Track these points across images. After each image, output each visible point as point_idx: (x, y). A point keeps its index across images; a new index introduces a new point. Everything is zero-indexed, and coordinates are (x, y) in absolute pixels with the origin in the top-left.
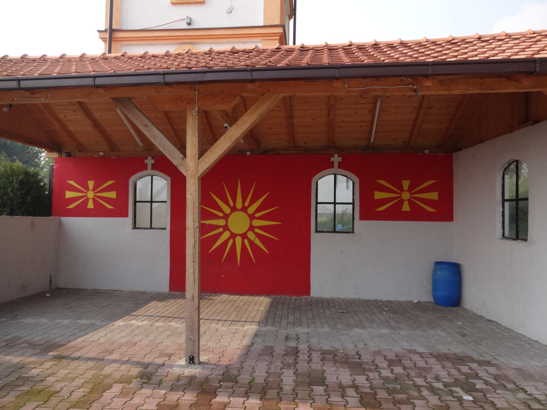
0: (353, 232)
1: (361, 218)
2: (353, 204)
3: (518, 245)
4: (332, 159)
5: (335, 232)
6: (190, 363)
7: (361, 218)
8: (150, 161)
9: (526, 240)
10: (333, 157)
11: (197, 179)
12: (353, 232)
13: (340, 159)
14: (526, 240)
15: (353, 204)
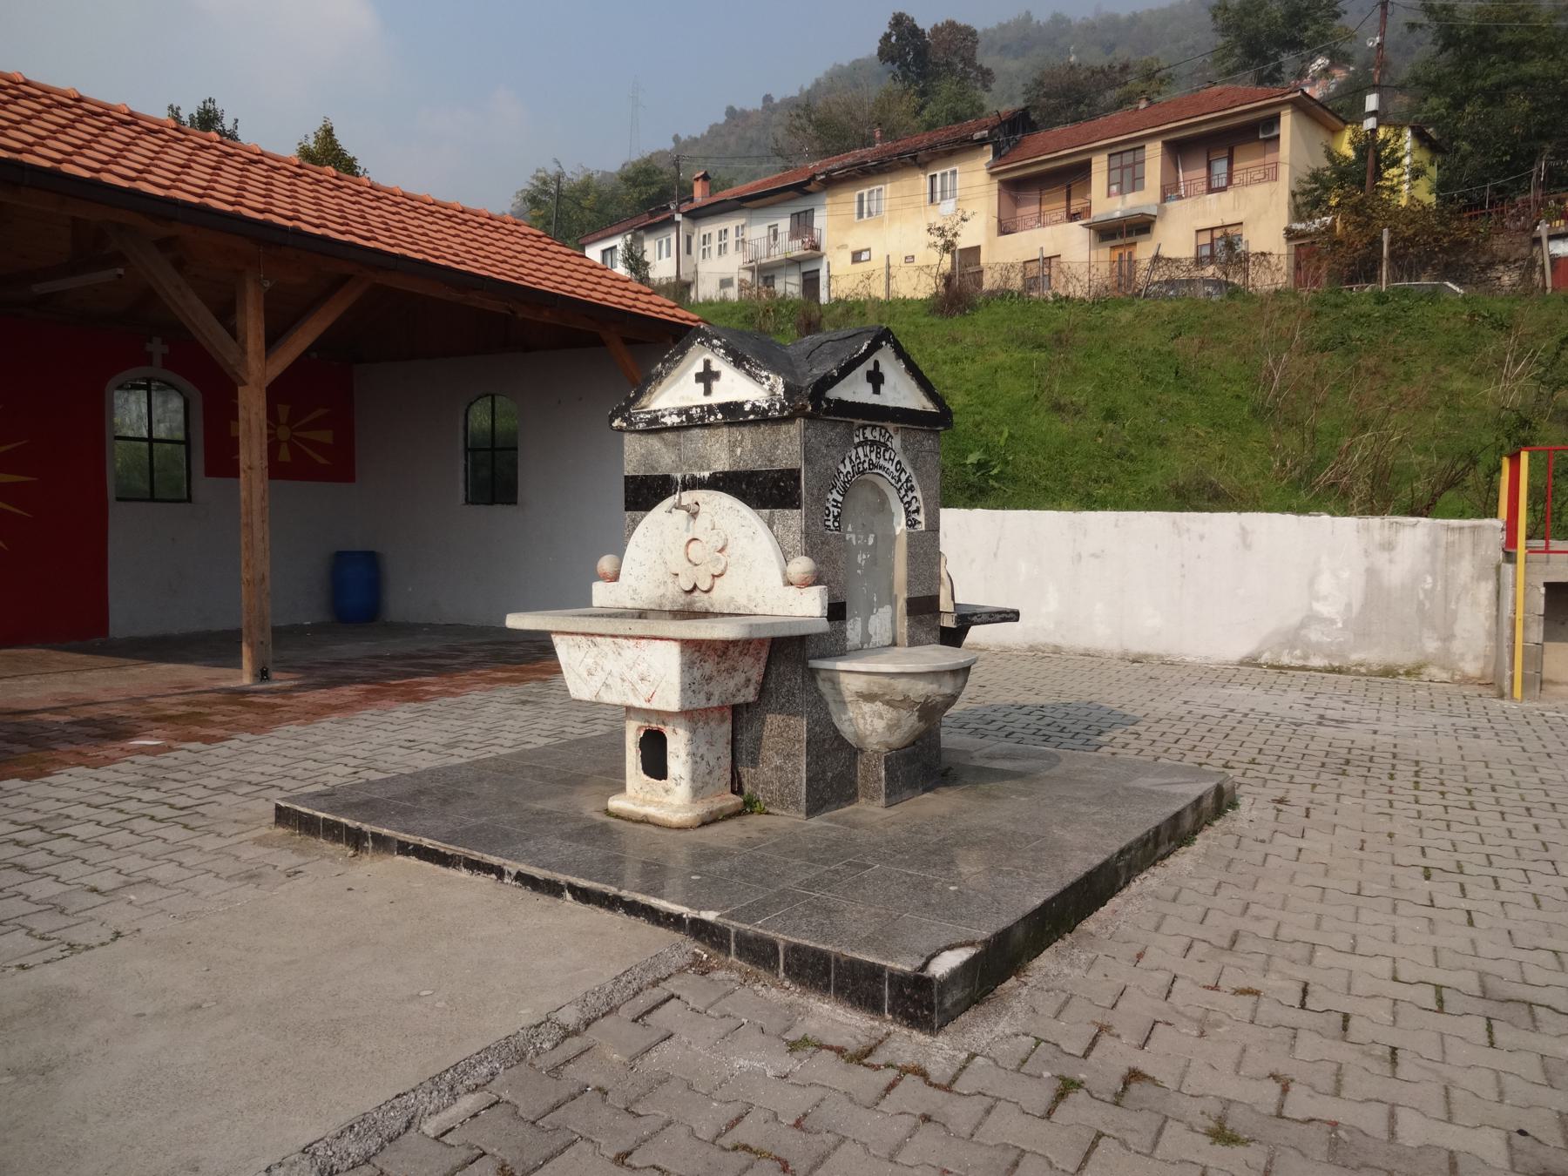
0: (189, 500)
1: (210, 472)
2: (187, 442)
3: (499, 511)
4: (149, 347)
5: (152, 499)
6: (262, 679)
7: (210, 472)
8: (157, 348)
9: (516, 503)
10: (151, 342)
11: (264, 390)
12: (189, 500)
13: (166, 349)
14: (516, 503)
15: (187, 442)
